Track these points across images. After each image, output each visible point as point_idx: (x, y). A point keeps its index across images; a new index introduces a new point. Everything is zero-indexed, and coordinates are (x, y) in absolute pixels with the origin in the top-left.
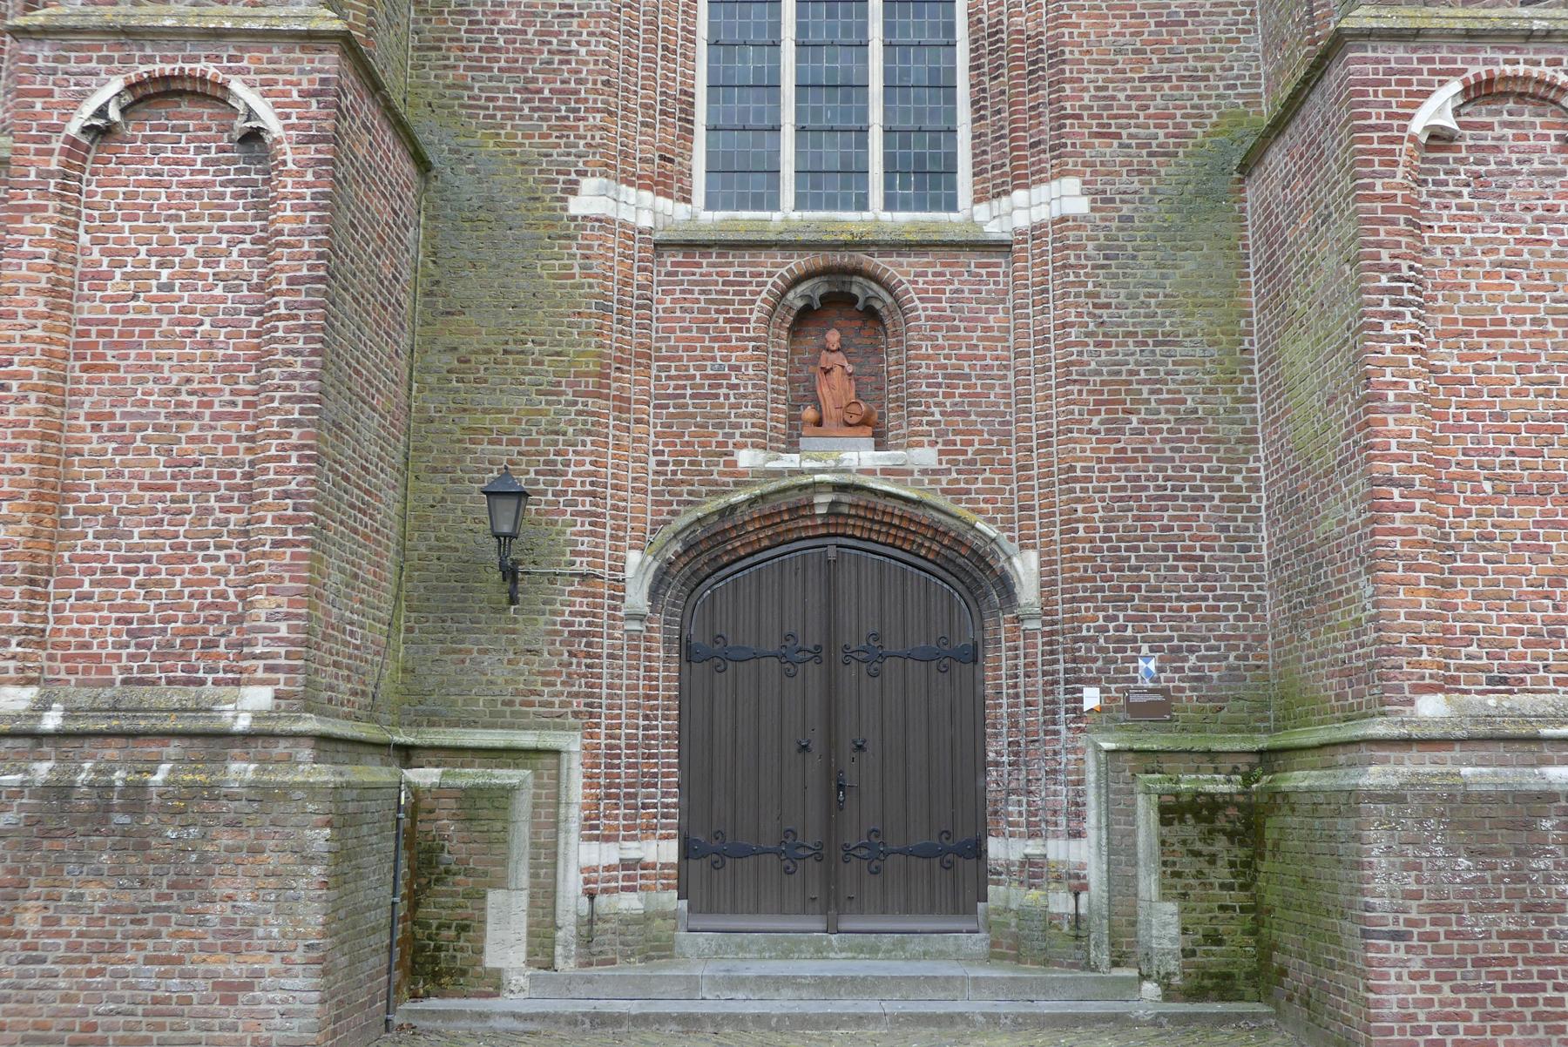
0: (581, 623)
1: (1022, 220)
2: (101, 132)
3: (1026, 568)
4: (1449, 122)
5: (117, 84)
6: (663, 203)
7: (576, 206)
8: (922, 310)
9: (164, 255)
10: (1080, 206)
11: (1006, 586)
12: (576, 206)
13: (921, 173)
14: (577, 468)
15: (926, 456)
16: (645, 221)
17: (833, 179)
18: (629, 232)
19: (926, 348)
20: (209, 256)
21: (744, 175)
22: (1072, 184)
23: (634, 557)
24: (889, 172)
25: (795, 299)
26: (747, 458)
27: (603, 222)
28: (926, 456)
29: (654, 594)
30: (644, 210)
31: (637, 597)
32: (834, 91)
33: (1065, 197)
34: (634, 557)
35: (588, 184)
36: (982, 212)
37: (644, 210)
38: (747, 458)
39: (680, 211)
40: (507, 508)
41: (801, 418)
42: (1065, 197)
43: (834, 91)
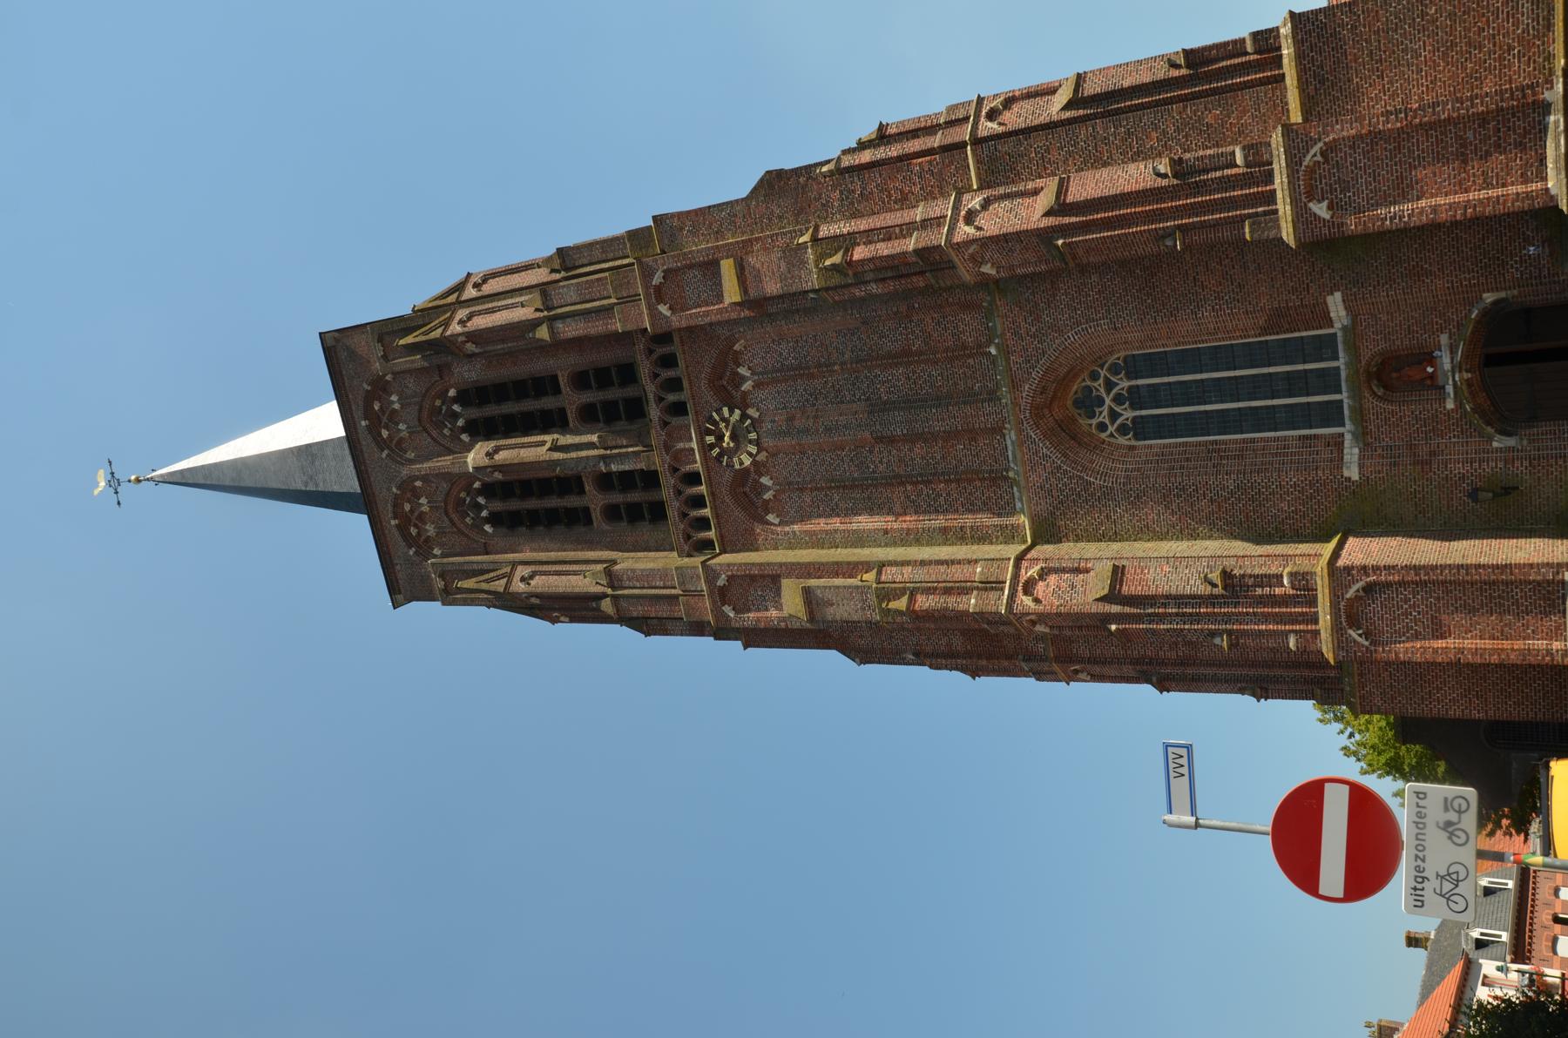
0: (1526, 463)
1: (1343, 313)
2: (1367, 635)
3: (1489, 297)
4: (1325, 203)
5: (1351, 632)
6: (1347, 444)
7: (1355, 476)
8: (1382, 345)
9: (1406, 614)
10: (1338, 295)
11: (1495, 303)
12: (1355, 476)
13: (1324, 348)
14: (1460, 469)
15: (1444, 339)
16: (1356, 451)
17: (1329, 381)
18: (1362, 458)
19: (1398, 343)
20: (1406, 601)
21: (1331, 414)
22: (1330, 299)
23: (1495, 444)
24: (1322, 360)
25: (1380, 392)
26: (1450, 405)
27: (1361, 466)
28: (1444, 339)
29: (1509, 435)
30: (1351, 453)
31: (1511, 442)
32: (1294, 384)
33: (1336, 304)
34: (1495, 444)
35: (1346, 473)
36: (1338, 325)
37: (1351, 453)
38: (1450, 405)
39: (1348, 437)
40: (1482, 495)
41: (1433, 385)
42: (1336, 304)
43: (1294, 384)
